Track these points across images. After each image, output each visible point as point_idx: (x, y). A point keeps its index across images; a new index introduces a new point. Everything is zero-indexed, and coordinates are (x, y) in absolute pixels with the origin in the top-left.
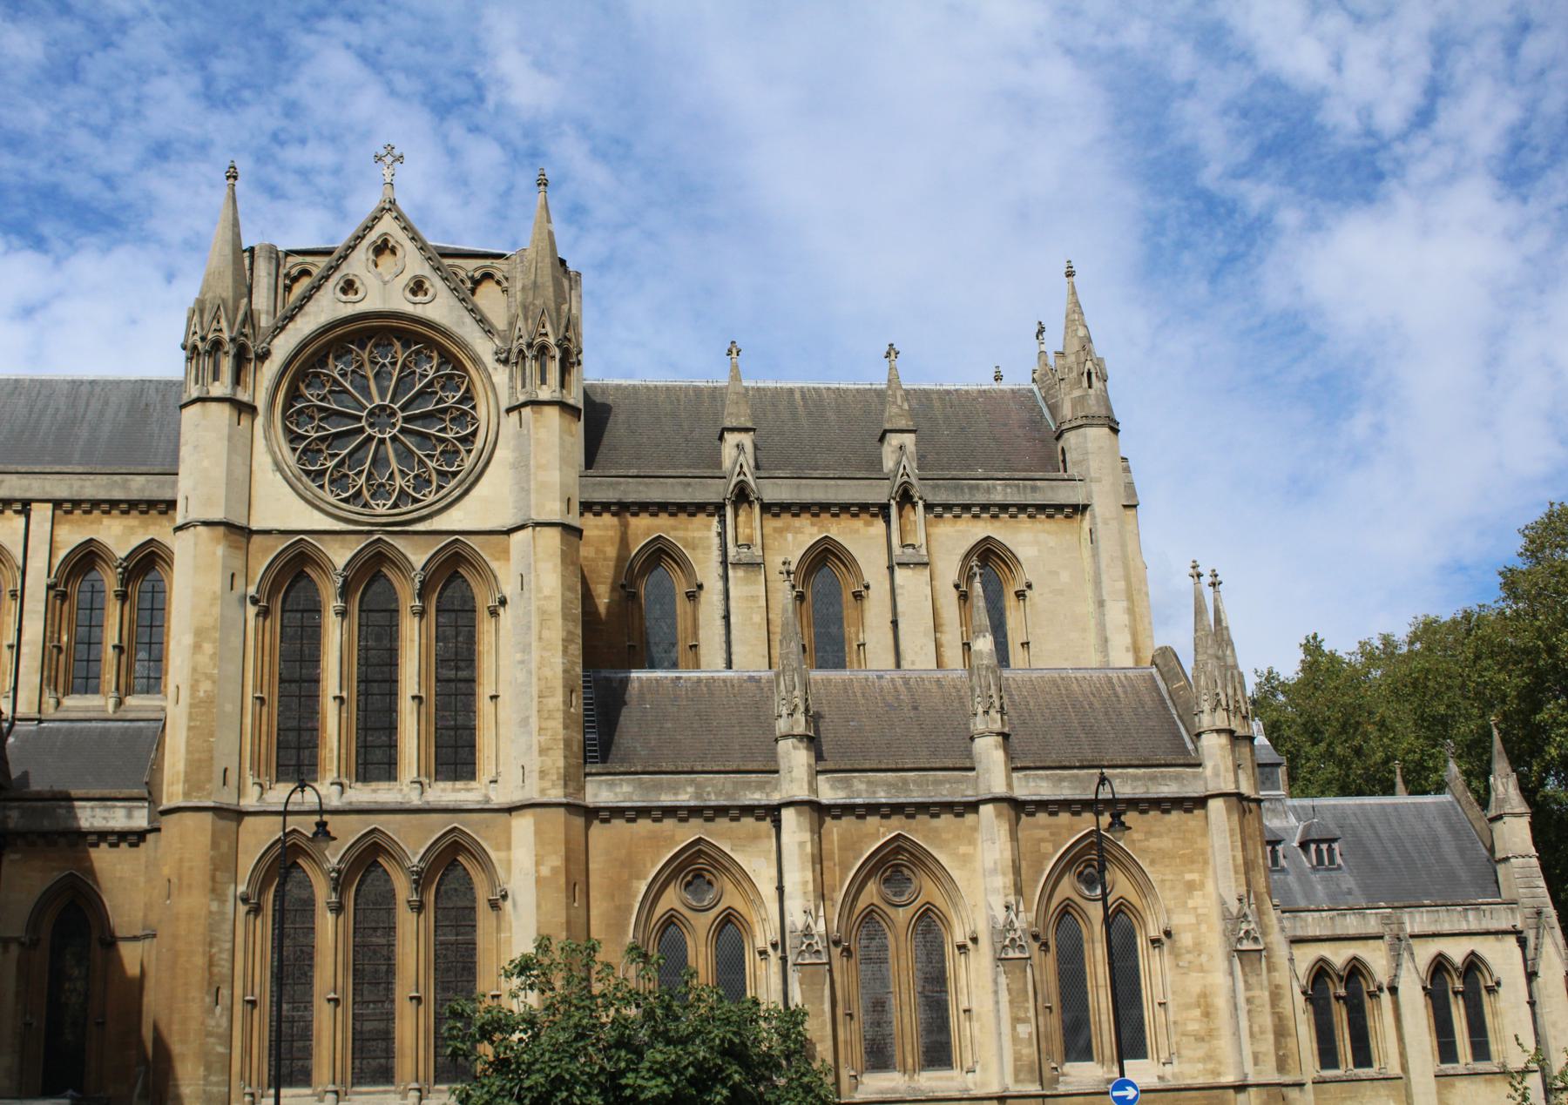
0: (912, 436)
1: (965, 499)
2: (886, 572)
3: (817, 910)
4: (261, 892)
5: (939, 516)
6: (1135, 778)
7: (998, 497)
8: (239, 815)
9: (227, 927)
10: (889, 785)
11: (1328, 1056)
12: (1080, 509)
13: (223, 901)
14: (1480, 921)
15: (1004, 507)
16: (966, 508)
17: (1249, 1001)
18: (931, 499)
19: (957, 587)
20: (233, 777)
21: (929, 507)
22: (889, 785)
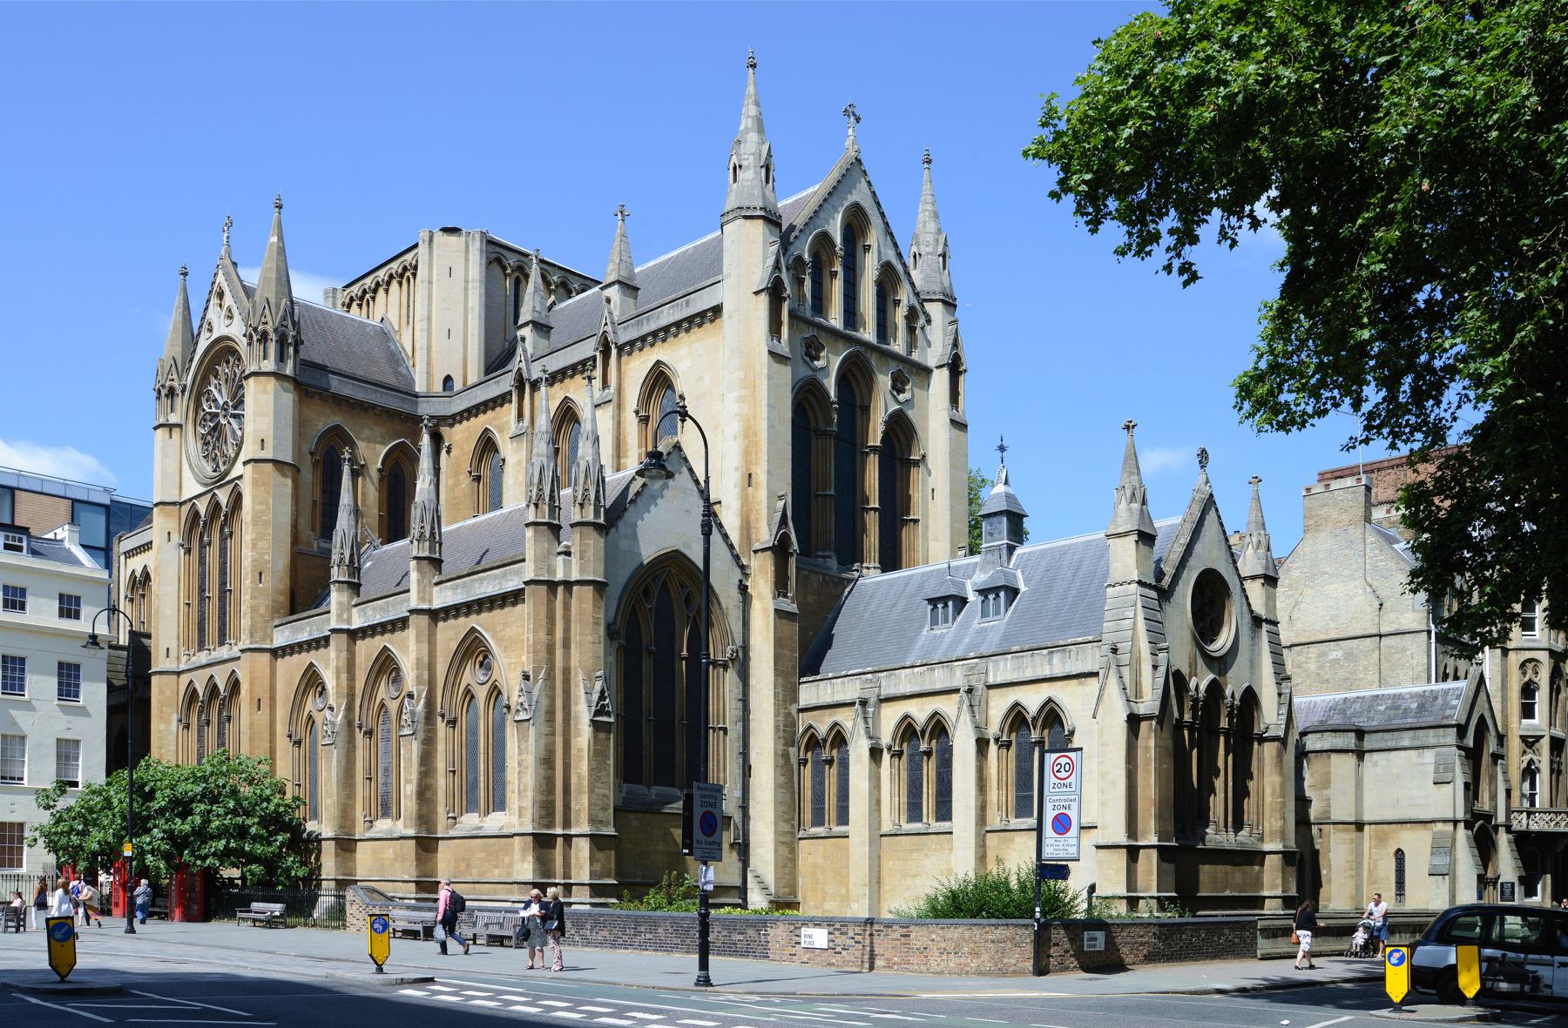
0: (616, 287)
1: (646, 329)
2: (967, 362)
3: (339, 706)
4: (188, 716)
5: (630, 354)
6: (496, 577)
7: (664, 322)
8: (178, 674)
9: (172, 738)
10: (381, 608)
11: (915, 813)
12: (717, 311)
13: (168, 722)
14: (1063, 663)
15: (666, 329)
16: (643, 339)
17: (520, 764)
18: (623, 338)
19: (637, 412)
20: (173, 653)
21: (620, 349)
22: (381, 608)
